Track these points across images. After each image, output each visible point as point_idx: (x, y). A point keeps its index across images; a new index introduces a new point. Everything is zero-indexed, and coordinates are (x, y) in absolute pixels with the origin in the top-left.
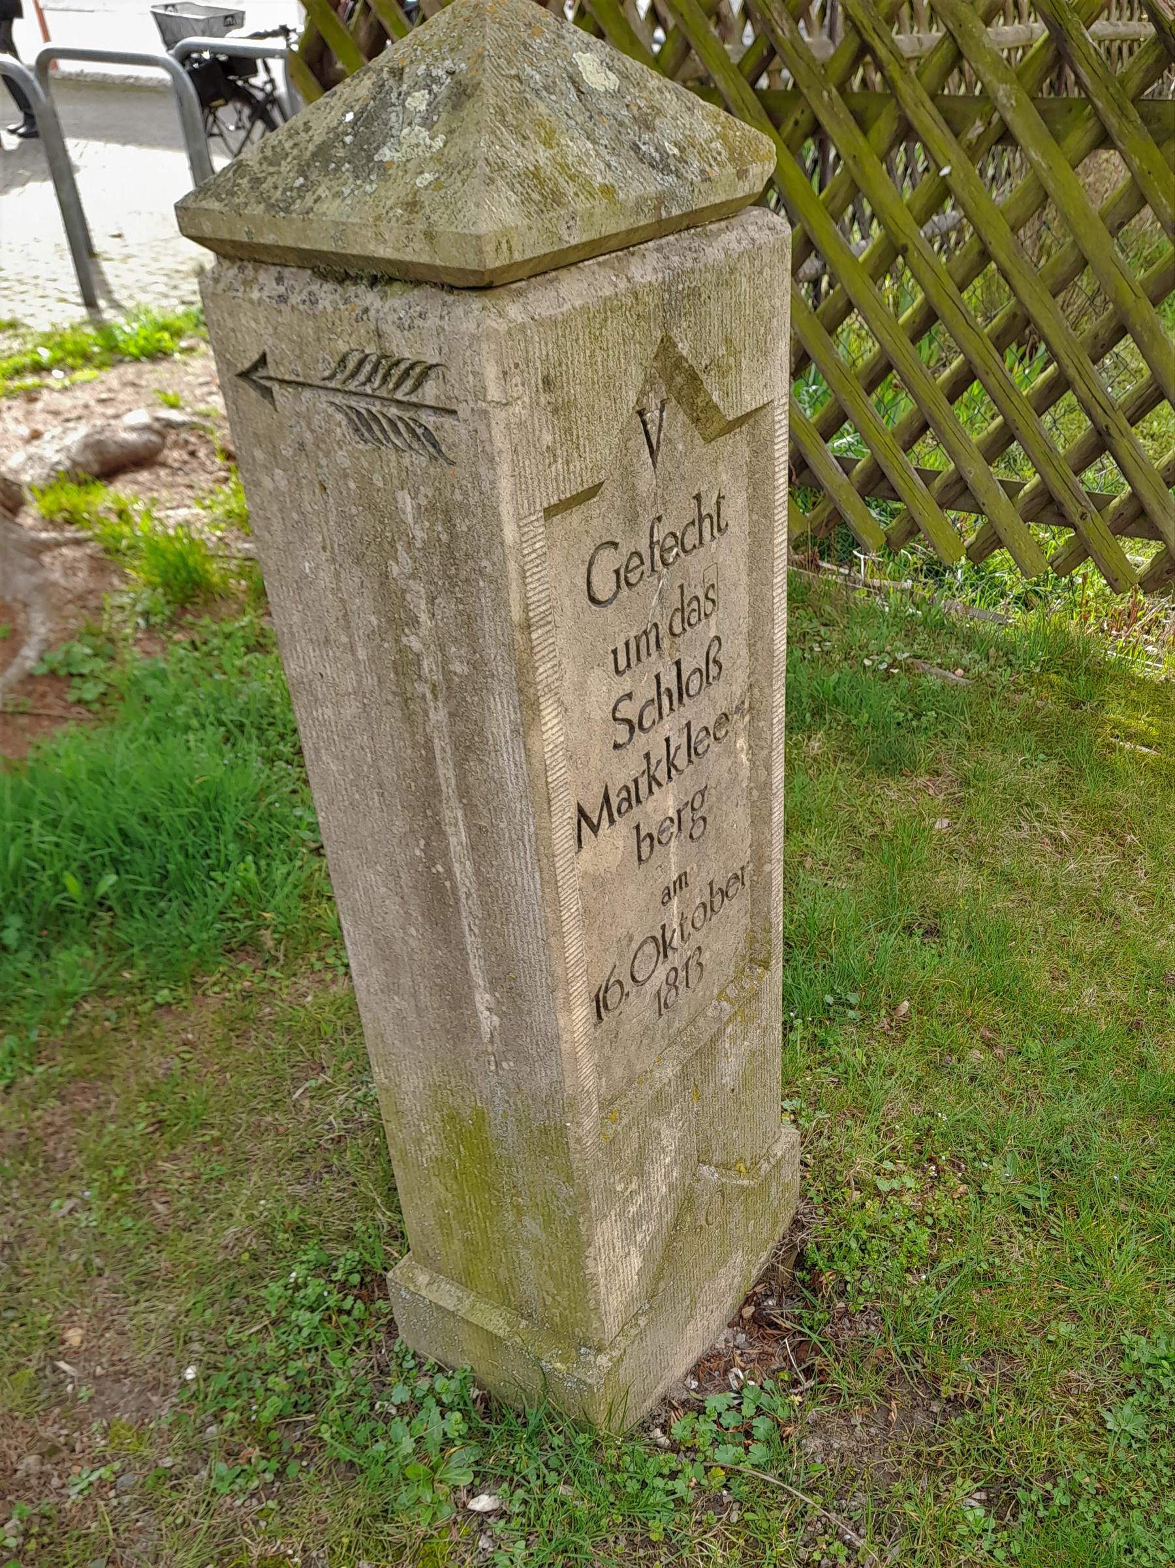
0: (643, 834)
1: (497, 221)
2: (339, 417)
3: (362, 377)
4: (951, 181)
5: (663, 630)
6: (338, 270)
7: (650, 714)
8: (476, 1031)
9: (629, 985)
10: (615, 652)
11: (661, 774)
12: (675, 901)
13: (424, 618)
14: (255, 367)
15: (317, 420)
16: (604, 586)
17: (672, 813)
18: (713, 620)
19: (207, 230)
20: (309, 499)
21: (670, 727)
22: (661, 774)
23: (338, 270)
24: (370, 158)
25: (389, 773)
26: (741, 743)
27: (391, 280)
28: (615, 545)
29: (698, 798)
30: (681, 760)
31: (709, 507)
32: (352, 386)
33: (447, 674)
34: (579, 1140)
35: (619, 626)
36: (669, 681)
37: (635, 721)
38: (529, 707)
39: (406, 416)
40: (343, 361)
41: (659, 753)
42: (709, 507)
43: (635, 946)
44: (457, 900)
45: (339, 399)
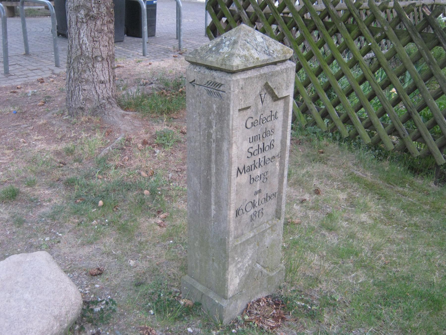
0: (252, 177)
1: (237, 63)
2: (205, 91)
3: (211, 85)
4: (371, 47)
5: (261, 136)
6: (210, 68)
7: (256, 152)
8: (210, 216)
9: (244, 211)
11: (257, 165)
12: (258, 195)
13: (214, 127)
14: (193, 82)
15: (201, 91)
16: (249, 125)
17: (259, 175)
18: (273, 136)
19: (189, 59)
20: (198, 104)
21: (260, 156)
22: (257, 165)
23: (210, 68)
24: (218, 51)
25: (202, 157)
26: (277, 164)
27: (218, 70)
28: (252, 118)
29: (266, 173)
30: (262, 164)
31: (274, 113)
32: (209, 86)
33: (217, 138)
34: (228, 242)
35: (251, 133)
36: (261, 146)
37: (253, 153)
38: (230, 144)
39: (217, 92)
40: (208, 82)
41: (257, 161)
42: (274, 113)
43: (247, 202)
44: (211, 184)
45: (206, 88)
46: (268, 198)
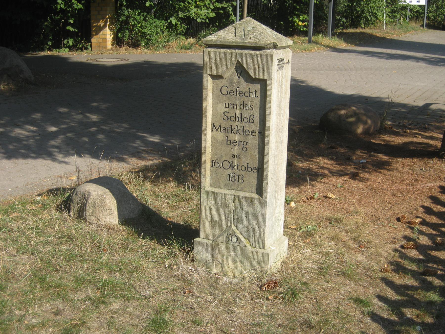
46: (250, 169)
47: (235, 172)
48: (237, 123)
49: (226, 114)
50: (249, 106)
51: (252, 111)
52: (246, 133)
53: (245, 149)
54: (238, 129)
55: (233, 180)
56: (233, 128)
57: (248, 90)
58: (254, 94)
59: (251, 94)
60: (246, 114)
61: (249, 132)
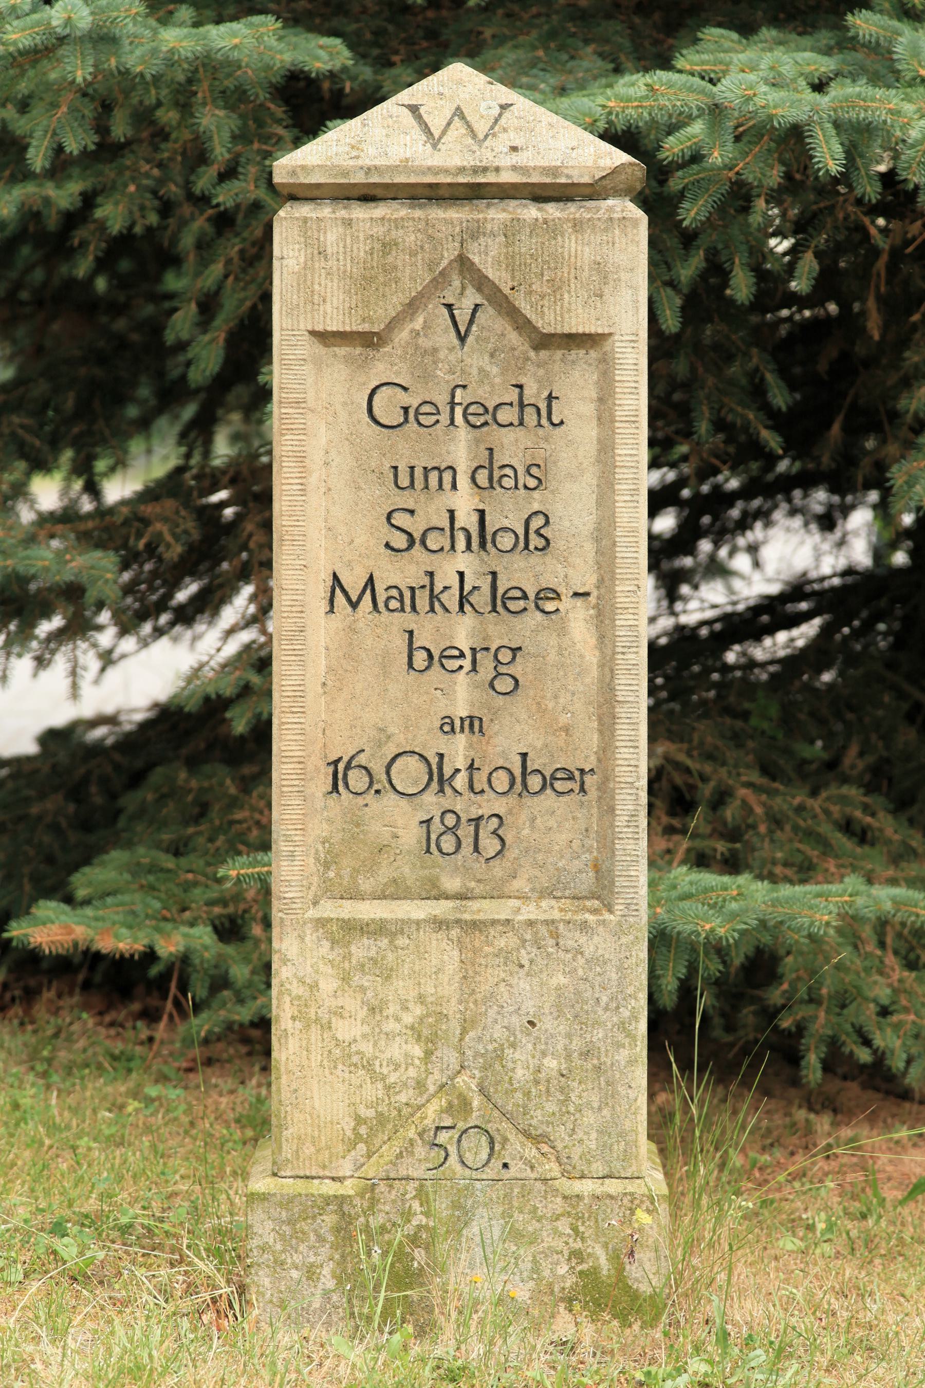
10: (396, 468)
37: (417, 536)
46: (535, 782)
47: (458, 808)
48: (463, 561)
49: (399, 519)
50: (521, 471)
51: (536, 494)
52: (512, 605)
53: (505, 685)
54: (467, 588)
55: (448, 844)
56: (438, 588)
57: (512, 396)
58: (544, 413)
59: (529, 411)
60: (508, 513)
61: (525, 597)
